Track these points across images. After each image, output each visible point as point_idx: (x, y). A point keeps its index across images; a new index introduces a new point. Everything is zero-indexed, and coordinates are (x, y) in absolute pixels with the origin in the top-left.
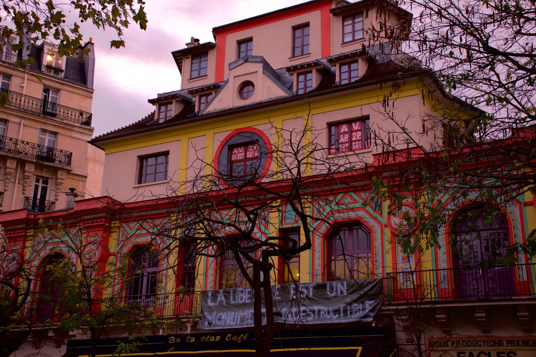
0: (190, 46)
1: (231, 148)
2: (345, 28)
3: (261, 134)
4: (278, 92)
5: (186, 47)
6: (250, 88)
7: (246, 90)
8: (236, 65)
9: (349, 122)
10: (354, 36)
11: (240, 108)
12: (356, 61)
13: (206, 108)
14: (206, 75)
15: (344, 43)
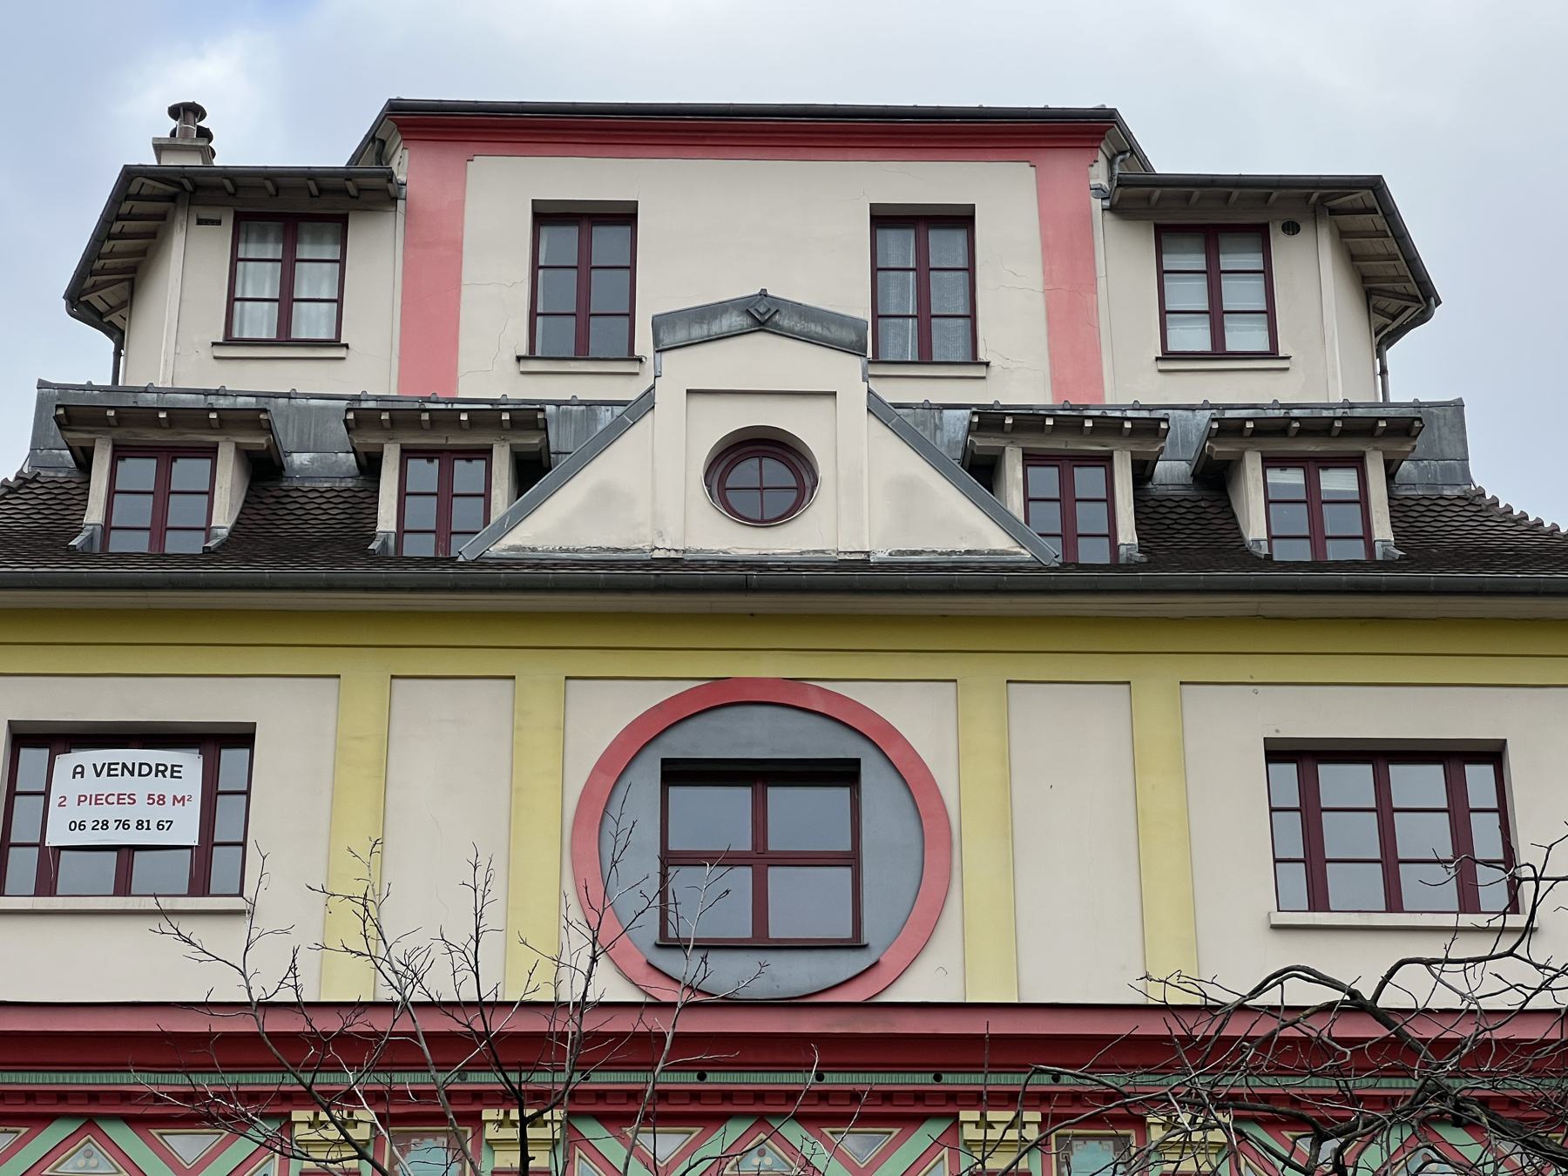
0: (172, 161)
1: (678, 773)
2: (1170, 284)
3: (880, 737)
4: (959, 526)
5: (151, 160)
6: (775, 472)
7: (746, 472)
8: (698, 332)
9: (1381, 755)
10: (1218, 334)
11: (726, 564)
12: (1356, 462)
13: (516, 518)
14: (336, 343)
15: (1167, 356)
